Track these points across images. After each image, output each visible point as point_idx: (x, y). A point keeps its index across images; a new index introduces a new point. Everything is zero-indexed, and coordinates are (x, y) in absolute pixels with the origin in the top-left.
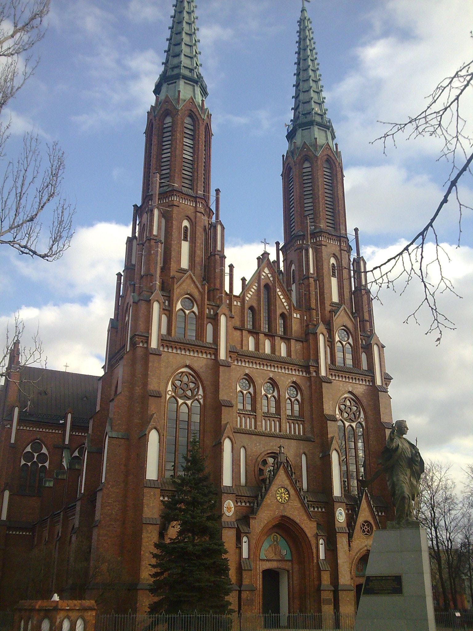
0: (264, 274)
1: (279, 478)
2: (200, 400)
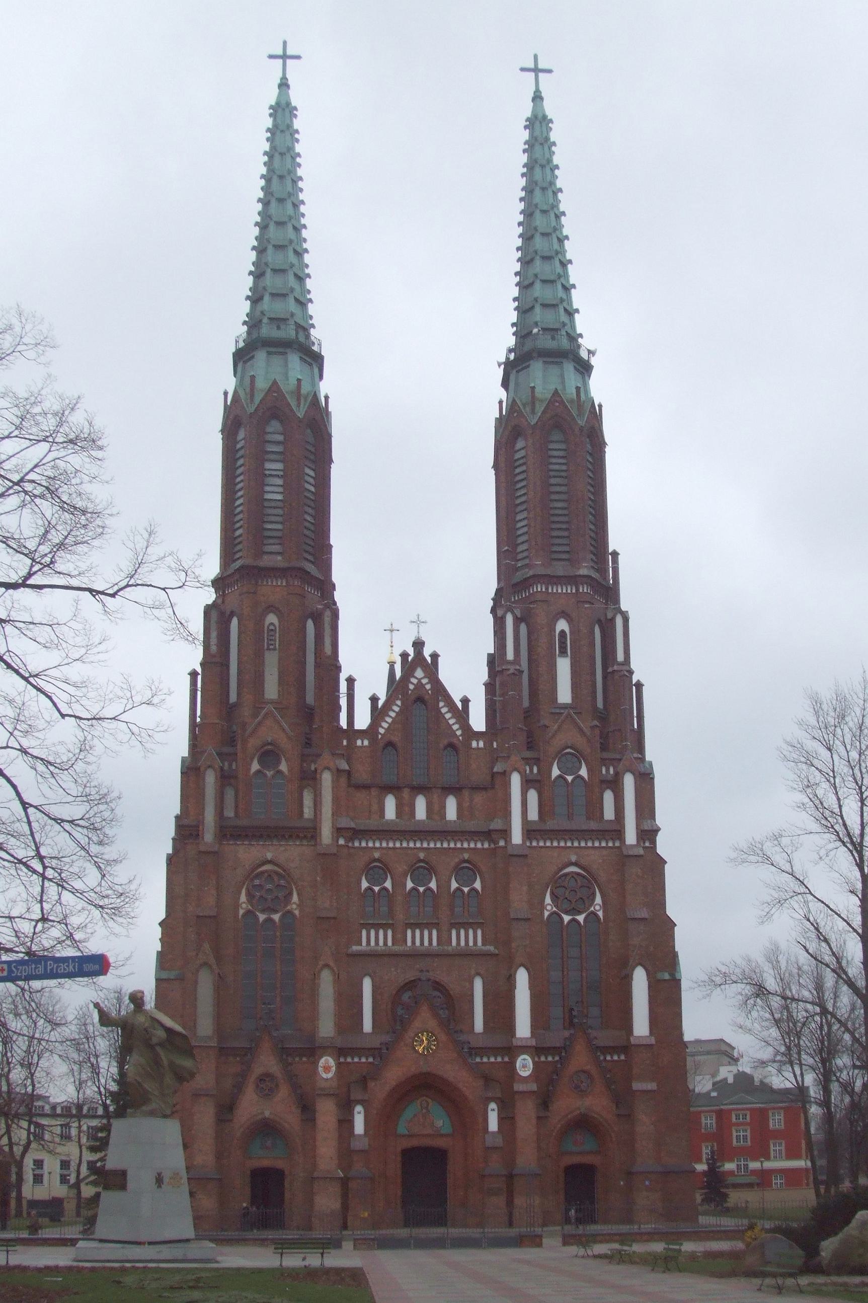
0: (414, 681)
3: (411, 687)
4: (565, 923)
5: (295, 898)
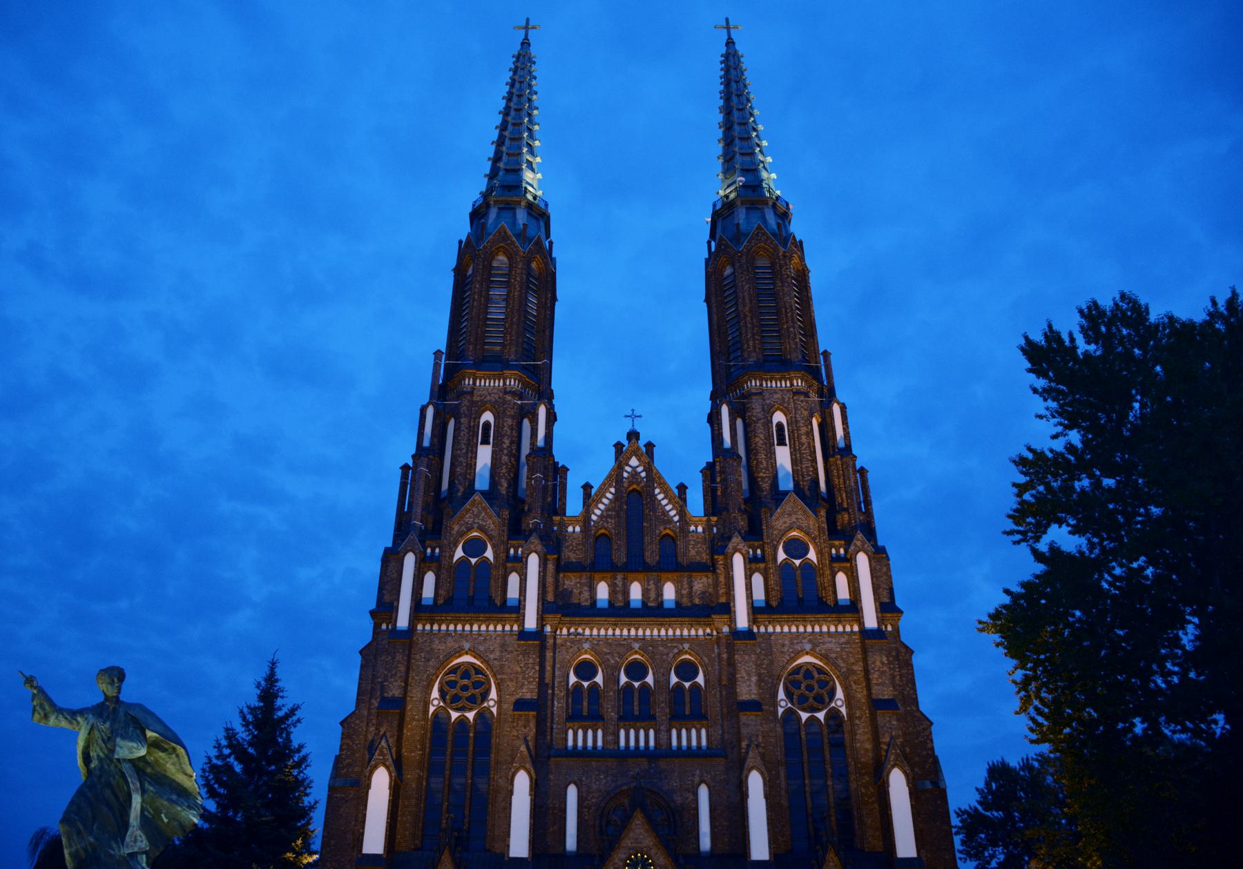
1: (631, 835)
2: (492, 709)
3: (625, 475)
4: (803, 721)
5: (493, 694)
